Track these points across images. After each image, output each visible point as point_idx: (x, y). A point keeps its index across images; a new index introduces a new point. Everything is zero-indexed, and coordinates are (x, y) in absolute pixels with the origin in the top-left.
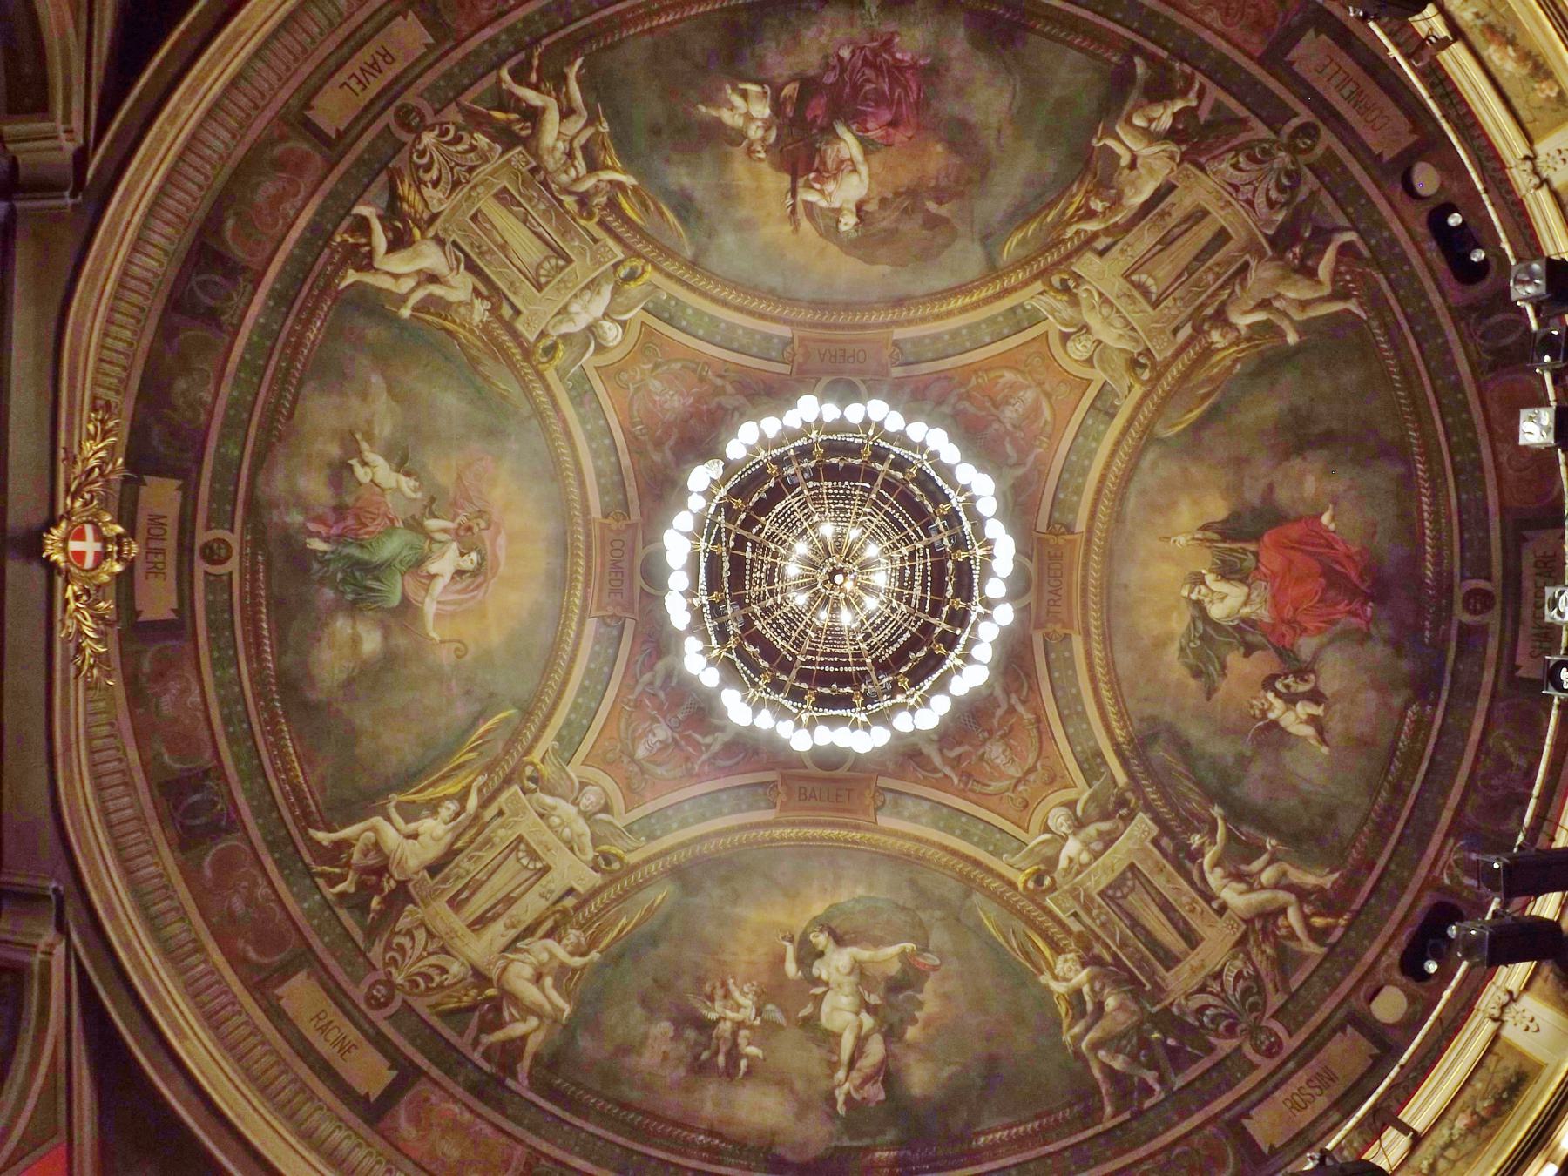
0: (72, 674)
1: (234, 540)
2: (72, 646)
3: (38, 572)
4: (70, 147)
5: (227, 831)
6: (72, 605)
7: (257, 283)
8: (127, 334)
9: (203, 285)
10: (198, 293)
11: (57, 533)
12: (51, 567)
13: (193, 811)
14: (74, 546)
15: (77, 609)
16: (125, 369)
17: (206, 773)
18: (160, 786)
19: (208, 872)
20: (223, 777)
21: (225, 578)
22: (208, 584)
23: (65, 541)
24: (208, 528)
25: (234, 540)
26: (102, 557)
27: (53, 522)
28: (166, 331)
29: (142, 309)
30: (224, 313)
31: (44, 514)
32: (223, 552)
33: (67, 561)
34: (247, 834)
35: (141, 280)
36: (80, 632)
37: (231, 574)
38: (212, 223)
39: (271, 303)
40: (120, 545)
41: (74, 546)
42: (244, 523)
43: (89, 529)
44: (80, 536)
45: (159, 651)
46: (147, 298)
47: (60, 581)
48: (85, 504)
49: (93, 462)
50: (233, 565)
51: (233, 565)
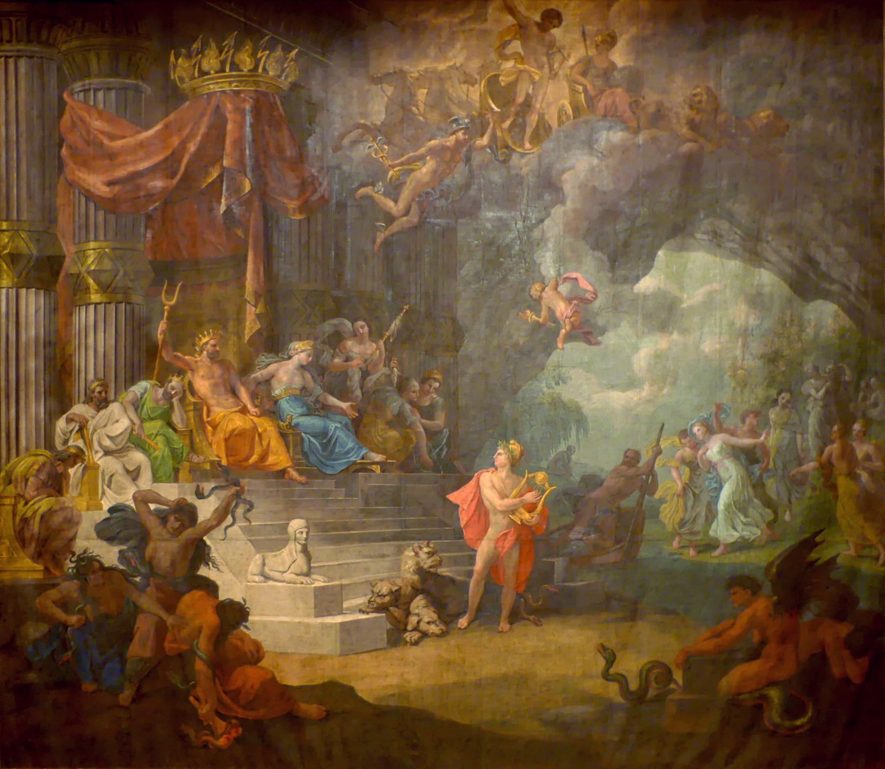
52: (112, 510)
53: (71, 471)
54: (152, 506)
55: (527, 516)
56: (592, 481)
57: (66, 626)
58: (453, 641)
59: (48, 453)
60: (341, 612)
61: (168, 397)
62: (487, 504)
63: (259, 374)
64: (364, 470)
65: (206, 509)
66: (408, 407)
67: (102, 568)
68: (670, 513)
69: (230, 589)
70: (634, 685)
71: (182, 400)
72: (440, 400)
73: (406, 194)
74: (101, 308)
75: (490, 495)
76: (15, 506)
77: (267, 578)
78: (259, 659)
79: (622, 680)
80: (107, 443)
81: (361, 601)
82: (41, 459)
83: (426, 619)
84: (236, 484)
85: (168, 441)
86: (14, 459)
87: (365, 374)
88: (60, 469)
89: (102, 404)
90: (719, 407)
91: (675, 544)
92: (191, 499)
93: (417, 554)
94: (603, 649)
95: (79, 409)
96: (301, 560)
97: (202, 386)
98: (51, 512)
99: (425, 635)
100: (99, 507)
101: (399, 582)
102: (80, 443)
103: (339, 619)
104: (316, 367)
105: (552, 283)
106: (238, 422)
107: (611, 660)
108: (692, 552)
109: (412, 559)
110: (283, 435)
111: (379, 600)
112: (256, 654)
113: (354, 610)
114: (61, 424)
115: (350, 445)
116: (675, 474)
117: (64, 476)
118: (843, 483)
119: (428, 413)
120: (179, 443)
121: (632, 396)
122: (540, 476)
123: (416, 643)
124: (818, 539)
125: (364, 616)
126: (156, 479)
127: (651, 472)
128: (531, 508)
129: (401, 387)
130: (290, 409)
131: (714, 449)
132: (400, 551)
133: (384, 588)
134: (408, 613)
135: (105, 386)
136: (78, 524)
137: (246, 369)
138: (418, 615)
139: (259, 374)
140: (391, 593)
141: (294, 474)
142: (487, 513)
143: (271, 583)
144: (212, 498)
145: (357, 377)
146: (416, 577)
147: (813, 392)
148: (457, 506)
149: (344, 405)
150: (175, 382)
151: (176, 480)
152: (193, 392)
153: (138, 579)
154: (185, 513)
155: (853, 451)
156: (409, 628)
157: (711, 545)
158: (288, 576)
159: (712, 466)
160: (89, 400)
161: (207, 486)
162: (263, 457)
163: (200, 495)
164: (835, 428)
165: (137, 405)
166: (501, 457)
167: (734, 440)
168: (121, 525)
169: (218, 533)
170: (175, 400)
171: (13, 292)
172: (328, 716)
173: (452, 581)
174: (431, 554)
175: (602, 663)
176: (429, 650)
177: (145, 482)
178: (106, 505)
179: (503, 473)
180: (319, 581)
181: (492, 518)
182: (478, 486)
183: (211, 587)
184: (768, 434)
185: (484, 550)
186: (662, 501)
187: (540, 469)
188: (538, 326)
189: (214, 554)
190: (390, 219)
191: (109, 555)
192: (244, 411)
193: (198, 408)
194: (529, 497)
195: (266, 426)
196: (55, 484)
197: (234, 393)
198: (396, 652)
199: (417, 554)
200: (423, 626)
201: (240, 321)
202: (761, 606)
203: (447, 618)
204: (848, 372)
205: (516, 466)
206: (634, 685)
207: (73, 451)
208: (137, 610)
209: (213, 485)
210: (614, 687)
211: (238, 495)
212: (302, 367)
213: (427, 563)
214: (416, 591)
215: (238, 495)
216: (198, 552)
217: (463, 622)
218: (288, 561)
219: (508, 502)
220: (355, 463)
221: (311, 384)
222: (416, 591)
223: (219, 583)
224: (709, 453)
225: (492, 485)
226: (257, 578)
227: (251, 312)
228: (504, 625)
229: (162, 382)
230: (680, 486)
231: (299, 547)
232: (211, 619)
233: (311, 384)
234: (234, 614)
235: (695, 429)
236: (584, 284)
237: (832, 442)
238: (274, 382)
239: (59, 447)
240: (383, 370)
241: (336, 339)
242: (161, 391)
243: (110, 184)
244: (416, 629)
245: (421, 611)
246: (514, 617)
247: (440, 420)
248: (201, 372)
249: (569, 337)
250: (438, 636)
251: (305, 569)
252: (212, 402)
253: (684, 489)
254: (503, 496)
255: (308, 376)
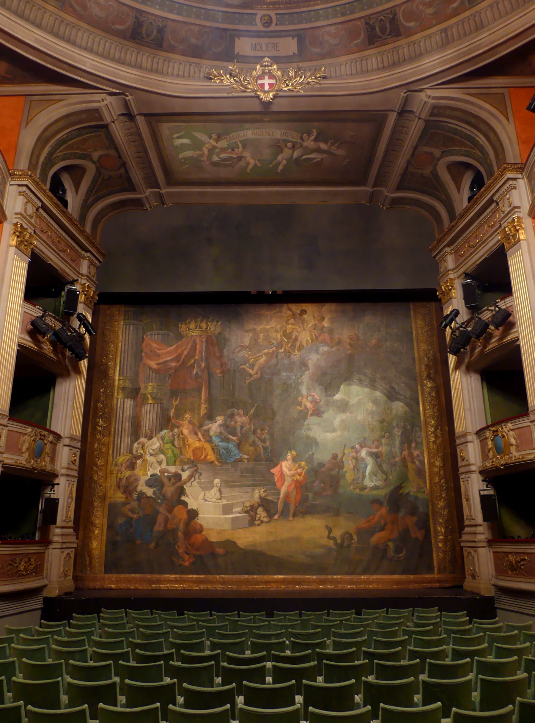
0: (318, 86)
1: (260, 13)
2: (307, 86)
3: (277, 100)
4: (109, 99)
5: (395, 14)
6: (290, 88)
7: (141, 12)
8: (176, 65)
9: (148, 36)
10: (152, 38)
11: (262, 96)
12: (275, 97)
13: (383, 30)
14: (267, 88)
15: (292, 84)
16: (190, 65)
17: (367, 24)
18: (369, 45)
19: (412, 24)
20: (369, 16)
21: (278, 16)
22: (280, 24)
23: (265, 92)
24: (256, 25)
25: (260, 13)
26: (272, 77)
27: (258, 97)
28: (172, 50)
29: (165, 60)
30: (159, 26)
31: (256, 99)
32: (266, 18)
33: (272, 91)
34: (397, 6)
35: (153, 62)
36: (301, 83)
37: (276, 14)
38: (121, 35)
39: (149, 3)
40: (265, 66)
41: (267, 88)
42: (253, 9)
43: (260, 82)
44: (263, 85)
45: (310, 45)
46: (159, 59)
47: (280, 94)
48: (249, 83)
49: (232, 80)
50: (272, 13)
51: (272, 13)
52: (151, 476)
53: (138, 461)
54: (166, 474)
55: (298, 477)
56: (321, 465)
57: (132, 519)
58: (272, 524)
59: (130, 455)
60: (232, 514)
61: (173, 435)
62: (284, 473)
63: (205, 428)
64: (242, 461)
65: (185, 475)
66: (257, 439)
67: (147, 497)
68: (349, 476)
69: (192, 504)
70: (339, 541)
71: (178, 437)
72: (268, 436)
73: (256, 368)
74: (152, 405)
75: (285, 470)
76: (117, 474)
77: (206, 500)
78: (202, 532)
79: (334, 539)
80: (151, 451)
81: (239, 509)
82: (128, 457)
83: (263, 516)
84: (196, 466)
85: (173, 451)
86: (118, 457)
87: (242, 428)
88: (134, 461)
89: (150, 438)
90: (364, 438)
91: (352, 487)
92: (180, 472)
93: (259, 492)
94: (327, 527)
95: (142, 440)
96: (218, 494)
97: (185, 432)
98: (130, 476)
99: (262, 522)
100: (147, 475)
101: (253, 502)
102: (142, 452)
103: (231, 516)
104: (225, 426)
105: (306, 397)
106: (197, 444)
107: (330, 531)
108: (358, 490)
109: (258, 493)
110: (213, 449)
111: (246, 509)
112: (201, 529)
113: (237, 513)
114: (136, 445)
115: (236, 452)
116: (350, 462)
117: (136, 463)
118: (410, 465)
119: (263, 441)
120: (177, 452)
121: (334, 434)
122: (303, 463)
123: (259, 525)
124: (403, 485)
125: (240, 515)
126: (168, 464)
127: (342, 461)
128: (300, 474)
129: (254, 432)
130: (216, 440)
131: (363, 453)
132: (253, 490)
133: (248, 504)
134: (256, 514)
135: (152, 432)
136: (139, 481)
137: (201, 426)
138: (260, 514)
139: (205, 428)
140: (250, 506)
141: (217, 463)
142: (284, 476)
143: (207, 502)
144: (187, 471)
145: (239, 429)
146: (259, 500)
147: (397, 433)
148: (274, 474)
149: (234, 438)
150: (176, 430)
151: (175, 465)
152: (182, 434)
153: (159, 501)
154: (177, 476)
155: (412, 454)
156: (257, 519)
157: (364, 488)
158: (213, 500)
159: (363, 459)
160: (146, 437)
161: (186, 467)
162: (206, 457)
163: (183, 470)
164: (406, 445)
165: (163, 438)
166: (289, 456)
167: (370, 450)
168: (155, 481)
169: (189, 484)
170: (176, 437)
171: (122, 400)
172: (227, 553)
173: (272, 501)
174: (264, 492)
175: (327, 533)
176: (263, 528)
177: (164, 466)
178: (149, 474)
179: (290, 462)
180: (224, 502)
181: (286, 478)
182: (281, 466)
183: (185, 504)
184: (382, 448)
185: (283, 490)
186: (346, 472)
187: (302, 461)
188: (301, 411)
189: (187, 492)
190: (251, 376)
191: (150, 492)
192: (200, 440)
193: (184, 440)
194: (299, 471)
195: (207, 446)
196: (132, 466)
197: (196, 434)
198: (252, 529)
199: (259, 492)
200: (262, 519)
201: (199, 410)
202: (384, 511)
203: (270, 515)
204: (408, 426)
205: (294, 460)
206: (339, 541)
207: (139, 454)
208: (158, 512)
209: (188, 466)
210: (332, 542)
211: (196, 470)
212: (220, 425)
213: (263, 495)
214: (259, 505)
215: (196, 470)
216: (181, 491)
217: (276, 517)
218: (213, 494)
219: (292, 472)
220: (238, 459)
221: (223, 431)
222: (259, 505)
223: (188, 502)
224: (362, 455)
225: (286, 466)
226: (202, 501)
227: (203, 406)
228: (291, 518)
229: (172, 430)
230: (352, 466)
231: (218, 489)
232: (185, 516)
233: (223, 431)
234: (193, 514)
235: (357, 446)
236: (317, 397)
237: (405, 450)
238: (210, 431)
239: (134, 453)
240: (248, 426)
241: (232, 416)
242: (171, 433)
243: (158, 364)
244: (258, 520)
245: (261, 513)
246: (294, 515)
247: (268, 444)
248: (186, 427)
249: (312, 415)
250: (267, 522)
251: (219, 497)
252: (189, 437)
253: (354, 468)
254: (290, 470)
255: (222, 428)
